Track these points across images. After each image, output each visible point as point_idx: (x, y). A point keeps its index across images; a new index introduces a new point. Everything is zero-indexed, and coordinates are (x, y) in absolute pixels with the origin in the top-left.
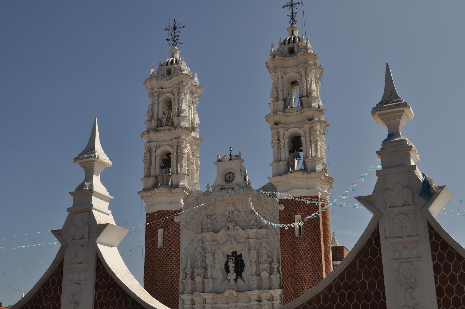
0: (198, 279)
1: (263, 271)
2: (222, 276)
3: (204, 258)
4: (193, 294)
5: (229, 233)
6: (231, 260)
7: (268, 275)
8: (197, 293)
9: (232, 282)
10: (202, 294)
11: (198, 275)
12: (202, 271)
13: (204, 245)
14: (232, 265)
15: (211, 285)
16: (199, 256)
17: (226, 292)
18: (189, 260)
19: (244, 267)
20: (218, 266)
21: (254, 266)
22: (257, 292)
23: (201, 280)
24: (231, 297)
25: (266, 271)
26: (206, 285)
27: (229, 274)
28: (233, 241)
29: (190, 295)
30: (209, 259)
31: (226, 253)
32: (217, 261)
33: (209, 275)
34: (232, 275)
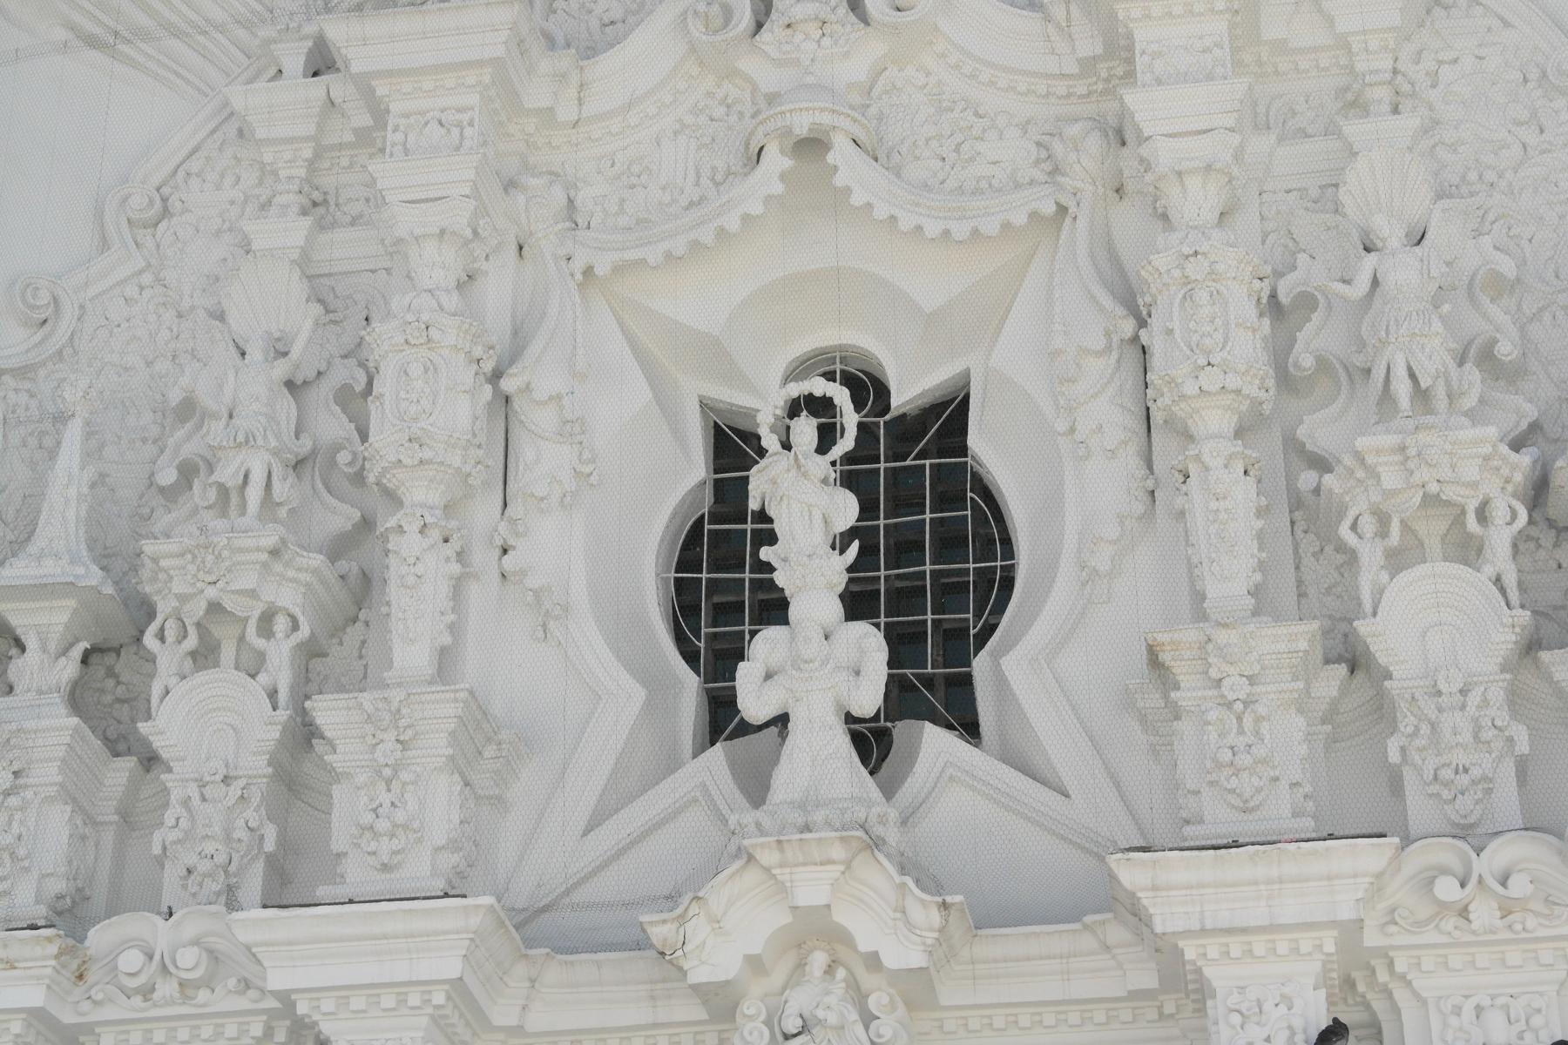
0: (208, 722)
1: (1397, 561)
2: (627, 696)
3: (331, 425)
4: (99, 937)
5: (761, 66)
6: (805, 429)
7: (1504, 629)
8: (160, 933)
9: (819, 757)
10: (255, 925)
11: (204, 656)
12: (288, 598)
13: (345, 249)
14: (808, 513)
15: (438, 806)
16: (255, 387)
17: (719, 893)
18: (73, 433)
19: (997, 588)
20: (554, 547)
21: (1229, 507)
22: (1340, 880)
23: (265, 729)
24: (800, 1000)
25: (1467, 550)
26: (348, 808)
27: (766, 645)
28: (840, 143)
29: (41, 949)
30: (425, 411)
31: (693, 388)
32: (544, 461)
33: (411, 654)
34: (819, 663)
